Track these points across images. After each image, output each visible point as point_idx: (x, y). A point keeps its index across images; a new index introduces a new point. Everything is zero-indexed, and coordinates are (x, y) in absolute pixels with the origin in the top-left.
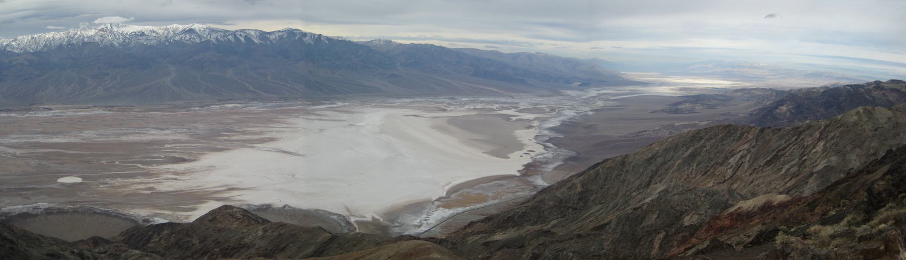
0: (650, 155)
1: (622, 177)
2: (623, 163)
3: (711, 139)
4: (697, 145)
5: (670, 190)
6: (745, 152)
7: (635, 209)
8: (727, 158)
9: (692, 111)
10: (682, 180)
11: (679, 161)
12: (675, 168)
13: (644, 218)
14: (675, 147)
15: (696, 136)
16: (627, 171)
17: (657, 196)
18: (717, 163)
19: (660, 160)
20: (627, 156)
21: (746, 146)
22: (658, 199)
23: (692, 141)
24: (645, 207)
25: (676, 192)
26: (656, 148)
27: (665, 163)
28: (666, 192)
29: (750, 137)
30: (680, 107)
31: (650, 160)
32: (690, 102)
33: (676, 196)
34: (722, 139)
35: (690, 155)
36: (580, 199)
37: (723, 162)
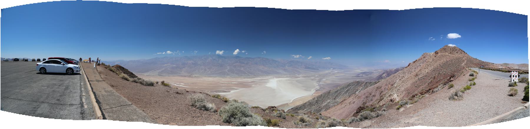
0: (337, 90)
1: (328, 97)
2: (329, 93)
3: (353, 86)
4: (349, 88)
5: (330, 102)
6: (361, 90)
7: (319, 107)
8: (356, 92)
9: (362, 76)
10: (343, 98)
11: (344, 92)
12: (342, 94)
13: (321, 110)
14: (343, 88)
15: (349, 85)
16: (330, 95)
17: (326, 104)
18: (353, 93)
19: (339, 92)
20: (330, 90)
21: (361, 88)
22: (327, 104)
23: (348, 86)
24: (322, 107)
25: (332, 102)
26: (339, 88)
27: (340, 93)
28: (329, 102)
29: (363, 85)
30: (359, 75)
31: (336, 92)
32: (362, 74)
33: (332, 104)
34: (356, 86)
35: (347, 91)
36: (316, 102)
37: (355, 93)
